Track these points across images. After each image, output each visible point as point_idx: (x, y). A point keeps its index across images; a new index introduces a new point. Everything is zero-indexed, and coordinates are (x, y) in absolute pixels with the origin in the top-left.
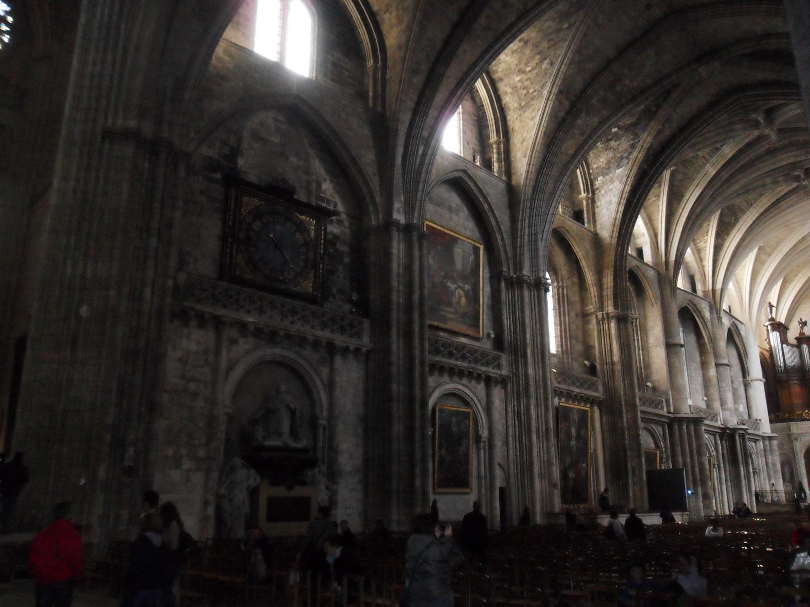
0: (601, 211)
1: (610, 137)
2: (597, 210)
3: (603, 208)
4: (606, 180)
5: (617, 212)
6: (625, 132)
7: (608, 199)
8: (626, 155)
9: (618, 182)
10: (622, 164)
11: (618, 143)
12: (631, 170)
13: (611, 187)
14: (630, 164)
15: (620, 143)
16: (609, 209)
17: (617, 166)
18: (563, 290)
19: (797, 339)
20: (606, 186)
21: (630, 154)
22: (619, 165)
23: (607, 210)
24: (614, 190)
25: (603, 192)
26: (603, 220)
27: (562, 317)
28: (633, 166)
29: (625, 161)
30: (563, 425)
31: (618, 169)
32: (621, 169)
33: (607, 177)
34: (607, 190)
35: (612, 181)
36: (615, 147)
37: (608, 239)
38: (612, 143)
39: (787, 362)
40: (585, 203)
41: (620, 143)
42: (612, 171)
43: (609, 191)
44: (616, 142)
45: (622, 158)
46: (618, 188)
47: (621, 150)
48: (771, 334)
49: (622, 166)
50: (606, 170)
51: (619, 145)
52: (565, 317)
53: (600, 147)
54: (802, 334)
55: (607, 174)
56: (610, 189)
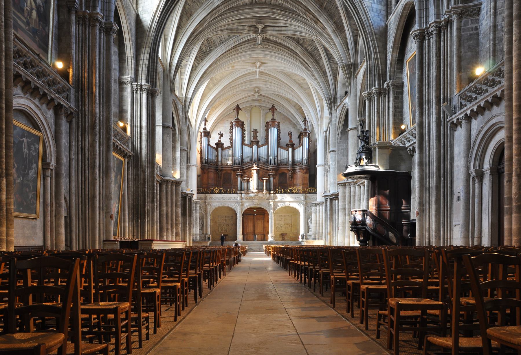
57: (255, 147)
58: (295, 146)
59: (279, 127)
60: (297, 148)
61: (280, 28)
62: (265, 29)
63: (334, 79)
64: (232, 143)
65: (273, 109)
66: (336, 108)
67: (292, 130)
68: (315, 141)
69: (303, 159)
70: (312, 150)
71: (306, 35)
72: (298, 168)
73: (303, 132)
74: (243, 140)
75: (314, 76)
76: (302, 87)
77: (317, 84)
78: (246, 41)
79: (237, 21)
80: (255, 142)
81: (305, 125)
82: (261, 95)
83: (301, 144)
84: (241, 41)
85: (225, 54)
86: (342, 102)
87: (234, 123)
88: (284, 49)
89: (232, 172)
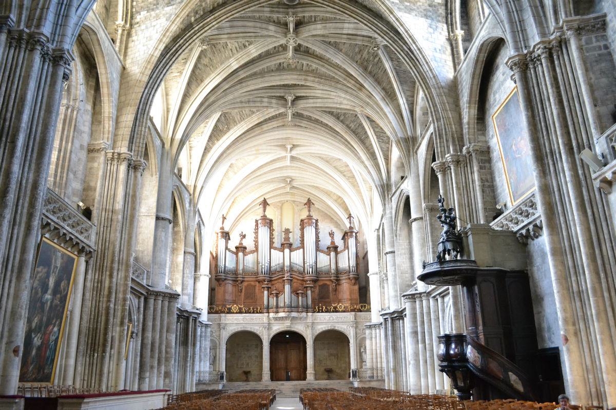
2: (131, 45)
9: (165, 19)
10: (172, 3)
12: (183, 10)
14: (183, 4)
17: (167, 4)
18: (72, 111)
19: (237, 248)
20: (149, 22)
22: (170, 3)
23: (144, 46)
24: (158, 26)
25: (143, 27)
27: (64, 143)
28: (186, 6)
30: (39, 269)
32: (171, 7)
35: (157, 17)
39: (227, 265)
40: (120, 32)
42: (160, 8)
43: (151, 26)
46: (162, 25)
48: (219, 240)
49: (173, 5)
52: (67, 142)
54: (241, 244)
55: (153, 10)
56: (152, 25)
57: (287, 251)
58: (339, 250)
59: (317, 225)
60: (341, 251)
63: (385, 162)
65: (309, 203)
66: (390, 197)
67: (335, 230)
68: (365, 243)
69: (349, 266)
70: (361, 255)
71: (348, 107)
72: (344, 278)
73: (348, 231)
75: (359, 158)
76: (344, 175)
77: (364, 168)
80: (287, 245)
81: (350, 223)
82: (293, 187)
83: (346, 247)
86: (399, 187)
87: (259, 222)
88: (321, 127)
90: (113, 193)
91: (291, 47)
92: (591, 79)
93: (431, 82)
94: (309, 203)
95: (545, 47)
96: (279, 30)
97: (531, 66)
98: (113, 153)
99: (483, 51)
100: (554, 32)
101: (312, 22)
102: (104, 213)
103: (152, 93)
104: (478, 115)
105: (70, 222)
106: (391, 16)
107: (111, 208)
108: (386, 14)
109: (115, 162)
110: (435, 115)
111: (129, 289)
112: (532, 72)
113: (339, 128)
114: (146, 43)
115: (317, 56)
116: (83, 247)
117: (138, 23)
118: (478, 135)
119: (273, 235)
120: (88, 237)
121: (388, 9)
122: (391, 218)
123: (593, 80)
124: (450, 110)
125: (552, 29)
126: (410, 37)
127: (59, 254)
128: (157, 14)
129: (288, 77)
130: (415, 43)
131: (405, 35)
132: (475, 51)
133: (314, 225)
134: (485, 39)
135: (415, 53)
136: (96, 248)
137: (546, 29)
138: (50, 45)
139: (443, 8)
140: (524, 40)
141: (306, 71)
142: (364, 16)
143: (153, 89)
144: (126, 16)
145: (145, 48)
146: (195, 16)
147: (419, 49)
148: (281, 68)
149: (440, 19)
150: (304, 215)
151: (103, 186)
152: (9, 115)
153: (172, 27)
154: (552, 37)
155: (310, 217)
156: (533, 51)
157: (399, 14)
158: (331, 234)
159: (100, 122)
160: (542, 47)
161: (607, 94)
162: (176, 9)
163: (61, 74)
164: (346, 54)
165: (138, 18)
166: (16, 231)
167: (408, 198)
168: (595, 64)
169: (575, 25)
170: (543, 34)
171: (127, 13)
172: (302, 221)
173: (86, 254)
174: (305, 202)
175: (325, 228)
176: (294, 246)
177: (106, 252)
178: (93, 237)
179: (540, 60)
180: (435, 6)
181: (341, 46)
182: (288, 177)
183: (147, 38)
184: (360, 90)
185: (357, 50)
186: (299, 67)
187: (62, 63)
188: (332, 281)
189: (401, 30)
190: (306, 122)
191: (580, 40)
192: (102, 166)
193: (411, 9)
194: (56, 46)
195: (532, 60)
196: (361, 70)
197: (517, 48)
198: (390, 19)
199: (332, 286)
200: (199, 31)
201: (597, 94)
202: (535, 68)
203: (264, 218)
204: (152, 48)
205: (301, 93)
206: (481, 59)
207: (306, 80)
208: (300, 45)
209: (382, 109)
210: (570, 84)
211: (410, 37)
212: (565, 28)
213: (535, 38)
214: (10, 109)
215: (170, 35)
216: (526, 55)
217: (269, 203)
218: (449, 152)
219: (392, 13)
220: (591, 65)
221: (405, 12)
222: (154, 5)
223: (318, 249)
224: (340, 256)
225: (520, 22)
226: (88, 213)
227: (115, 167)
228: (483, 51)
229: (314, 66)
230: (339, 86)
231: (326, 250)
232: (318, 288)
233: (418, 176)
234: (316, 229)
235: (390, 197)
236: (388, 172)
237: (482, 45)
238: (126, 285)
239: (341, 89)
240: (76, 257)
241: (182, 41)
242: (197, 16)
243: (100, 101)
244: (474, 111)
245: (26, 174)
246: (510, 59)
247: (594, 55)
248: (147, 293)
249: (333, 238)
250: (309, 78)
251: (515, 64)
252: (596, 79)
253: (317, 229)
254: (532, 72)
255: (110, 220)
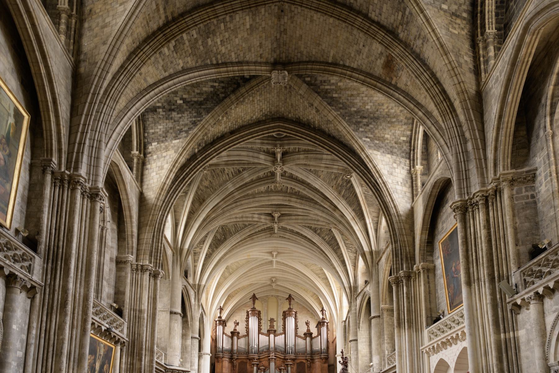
0: (150, 174)
1: (173, 107)
2: (146, 172)
3: (153, 172)
4: (161, 147)
5: (168, 178)
6: (189, 108)
7: (159, 164)
8: (186, 129)
9: (173, 151)
10: (179, 137)
11: (180, 115)
13: (164, 154)
15: (182, 116)
16: (159, 174)
17: (174, 137)
20: (159, 153)
21: (190, 129)
22: (177, 137)
23: (156, 174)
24: (168, 157)
26: (151, 181)
29: (184, 134)
31: (175, 139)
32: (178, 141)
33: (162, 144)
34: (160, 156)
35: (167, 149)
36: (176, 119)
37: (154, 199)
38: (174, 114)
41: (182, 116)
42: (169, 141)
43: (162, 157)
44: (178, 114)
45: (181, 131)
46: (172, 157)
47: (181, 123)
49: (180, 138)
50: (165, 137)
51: (180, 118)
53: (161, 113)
57: (272, 336)
58: (313, 336)
61: (297, 217)
62: (281, 218)
64: (248, 332)
74: (260, 329)
78: (262, 230)
79: (252, 209)
80: (271, 331)
81: (323, 314)
83: (319, 334)
84: (257, 230)
85: (241, 243)
89: (248, 361)
90: (138, 296)
91: (278, 174)
92: (516, 223)
93: (393, 211)
94: (290, 298)
95: (483, 195)
96: (269, 158)
97: (470, 210)
98: (137, 265)
99: (436, 187)
100: (492, 183)
101: (296, 152)
102: (132, 312)
103: (166, 215)
104: (428, 239)
105: (108, 320)
106: (363, 153)
107: (138, 308)
108: (359, 151)
109: (139, 272)
110: (394, 238)
111: (154, 369)
112: (471, 215)
113: (316, 239)
114: (159, 172)
115: (299, 181)
116: (119, 339)
117: (150, 153)
118: (427, 255)
119: (260, 323)
120: (122, 331)
121: (360, 147)
122: (356, 313)
123: (517, 225)
124: (406, 235)
125: (490, 180)
126: (377, 172)
127: (102, 345)
128: (166, 146)
129: (275, 198)
130: (381, 177)
131: (373, 171)
132: (429, 187)
133: (294, 316)
134: (438, 178)
135: (381, 186)
136: (127, 339)
137: (486, 179)
138: (87, 184)
139: (408, 144)
140: (467, 187)
141: (290, 193)
142: (340, 151)
143: (166, 211)
144: (140, 146)
145: (158, 176)
146: (198, 148)
147: (384, 183)
148: (270, 190)
149: (404, 154)
150: (286, 308)
151: (131, 291)
152: (61, 243)
153: (180, 159)
154: (489, 187)
155: (290, 310)
156: (473, 198)
157: (369, 152)
158: (307, 324)
159: (124, 239)
160: (480, 195)
161: (527, 236)
162: (182, 142)
163: (98, 208)
164: (324, 180)
165: (150, 148)
166: (74, 333)
167: (369, 299)
168: (521, 211)
169: (510, 177)
170: (483, 184)
171: (140, 143)
172: (284, 312)
173: (121, 344)
174: (287, 297)
175: (302, 319)
176: (278, 332)
177: (136, 342)
178: (125, 331)
179: (477, 205)
180: (400, 143)
181: (320, 173)
182: (273, 277)
183: (159, 167)
184: (335, 210)
185: (333, 177)
186: (284, 190)
187: (98, 199)
188: (308, 360)
189: (370, 166)
190: (289, 235)
191: (512, 190)
192: (129, 275)
193: (379, 147)
194: (92, 185)
195: (471, 205)
196: (336, 194)
197: (461, 195)
198: (362, 156)
199: (307, 364)
200: (202, 161)
201: (519, 235)
202: (473, 211)
203: (254, 309)
204: (164, 177)
205: (285, 211)
206: (434, 194)
207: (289, 201)
208: (285, 172)
209: (352, 227)
210: (499, 226)
211: (377, 172)
212: (501, 180)
213: (475, 188)
214: (62, 238)
215: (178, 165)
216: (467, 200)
217: (257, 297)
218: (402, 269)
219: (363, 151)
220: (518, 212)
221: (375, 150)
222: (163, 137)
223: (296, 335)
224: (314, 340)
225: (466, 171)
226: (119, 312)
227: (140, 276)
228: (436, 187)
229: (297, 189)
230: (317, 206)
231: (303, 336)
232: (296, 365)
233: (378, 283)
234: (295, 319)
235: (355, 296)
236: (355, 277)
237: (436, 183)
238: (152, 366)
239: (318, 209)
240: (114, 347)
241: (188, 170)
242: (200, 148)
243: (124, 221)
244: (425, 237)
245: (78, 290)
246: (453, 203)
247: (522, 203)
248: (165, 370)
249: (308, 326)
250: (292, 199)
251: (457, 208)
252: (520, 223)
253: (296, 319)
254: (471, 215)
255: (137, 317)
